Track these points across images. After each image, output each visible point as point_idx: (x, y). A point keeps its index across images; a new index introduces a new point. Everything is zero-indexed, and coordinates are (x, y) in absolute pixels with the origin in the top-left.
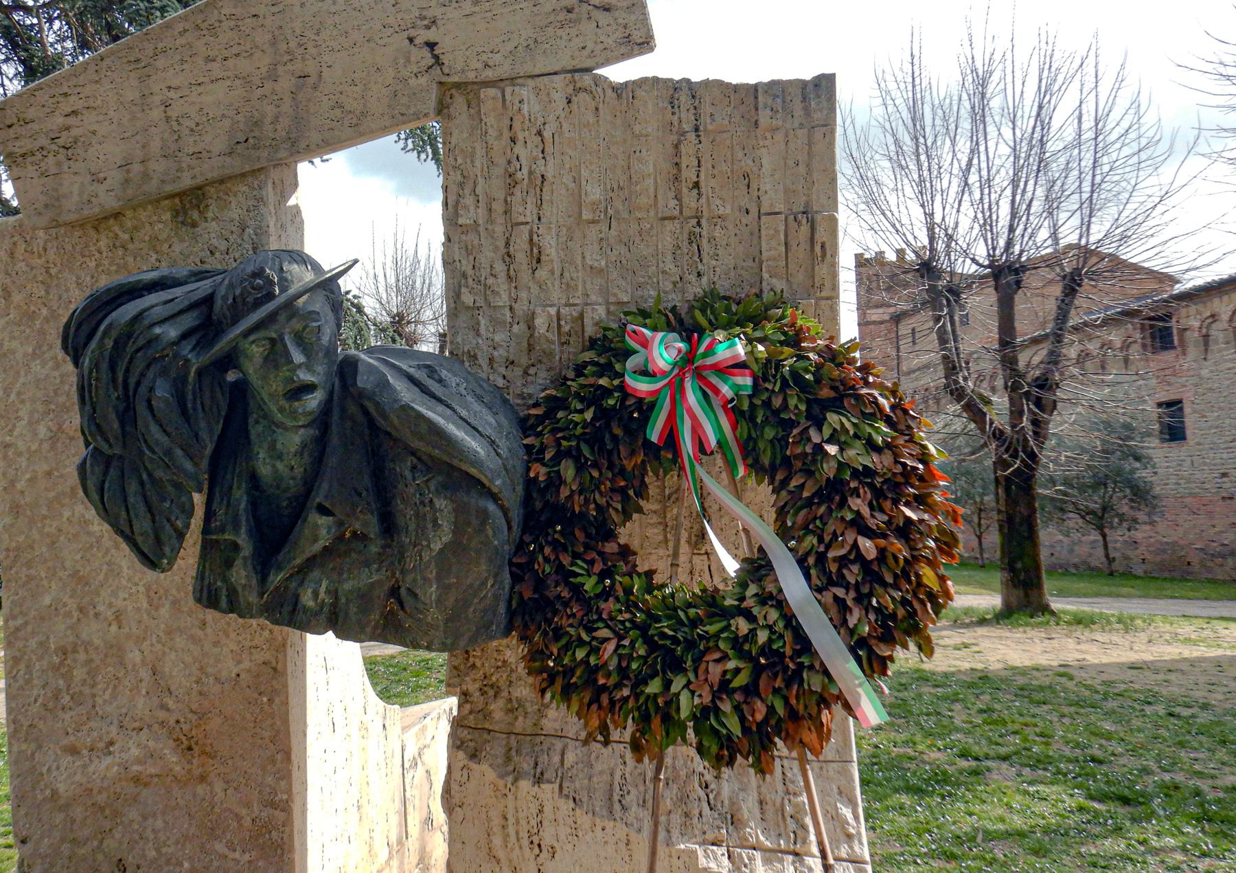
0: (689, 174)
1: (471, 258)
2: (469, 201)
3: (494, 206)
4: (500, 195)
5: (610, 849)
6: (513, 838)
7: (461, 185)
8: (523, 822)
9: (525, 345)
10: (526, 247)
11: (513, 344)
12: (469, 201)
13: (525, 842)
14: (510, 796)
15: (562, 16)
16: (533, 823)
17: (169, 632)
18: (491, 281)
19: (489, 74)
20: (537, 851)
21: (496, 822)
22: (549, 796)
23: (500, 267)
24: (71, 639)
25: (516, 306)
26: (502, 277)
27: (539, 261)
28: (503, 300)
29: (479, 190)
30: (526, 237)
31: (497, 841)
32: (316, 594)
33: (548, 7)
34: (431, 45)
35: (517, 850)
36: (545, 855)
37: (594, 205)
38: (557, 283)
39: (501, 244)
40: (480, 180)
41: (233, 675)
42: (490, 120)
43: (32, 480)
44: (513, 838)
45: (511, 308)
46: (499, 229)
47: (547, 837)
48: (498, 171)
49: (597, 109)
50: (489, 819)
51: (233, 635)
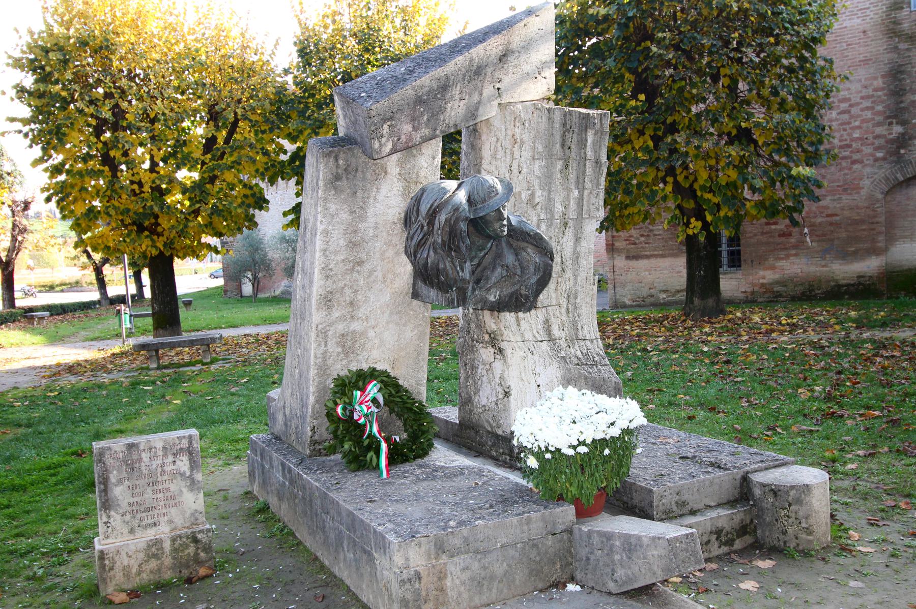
4: (510, 147)
21: (522, 368)
31: (523, 375)
42: (508, 118)
43: (337, 263)
47: (537, 371)
48: (509, 137)
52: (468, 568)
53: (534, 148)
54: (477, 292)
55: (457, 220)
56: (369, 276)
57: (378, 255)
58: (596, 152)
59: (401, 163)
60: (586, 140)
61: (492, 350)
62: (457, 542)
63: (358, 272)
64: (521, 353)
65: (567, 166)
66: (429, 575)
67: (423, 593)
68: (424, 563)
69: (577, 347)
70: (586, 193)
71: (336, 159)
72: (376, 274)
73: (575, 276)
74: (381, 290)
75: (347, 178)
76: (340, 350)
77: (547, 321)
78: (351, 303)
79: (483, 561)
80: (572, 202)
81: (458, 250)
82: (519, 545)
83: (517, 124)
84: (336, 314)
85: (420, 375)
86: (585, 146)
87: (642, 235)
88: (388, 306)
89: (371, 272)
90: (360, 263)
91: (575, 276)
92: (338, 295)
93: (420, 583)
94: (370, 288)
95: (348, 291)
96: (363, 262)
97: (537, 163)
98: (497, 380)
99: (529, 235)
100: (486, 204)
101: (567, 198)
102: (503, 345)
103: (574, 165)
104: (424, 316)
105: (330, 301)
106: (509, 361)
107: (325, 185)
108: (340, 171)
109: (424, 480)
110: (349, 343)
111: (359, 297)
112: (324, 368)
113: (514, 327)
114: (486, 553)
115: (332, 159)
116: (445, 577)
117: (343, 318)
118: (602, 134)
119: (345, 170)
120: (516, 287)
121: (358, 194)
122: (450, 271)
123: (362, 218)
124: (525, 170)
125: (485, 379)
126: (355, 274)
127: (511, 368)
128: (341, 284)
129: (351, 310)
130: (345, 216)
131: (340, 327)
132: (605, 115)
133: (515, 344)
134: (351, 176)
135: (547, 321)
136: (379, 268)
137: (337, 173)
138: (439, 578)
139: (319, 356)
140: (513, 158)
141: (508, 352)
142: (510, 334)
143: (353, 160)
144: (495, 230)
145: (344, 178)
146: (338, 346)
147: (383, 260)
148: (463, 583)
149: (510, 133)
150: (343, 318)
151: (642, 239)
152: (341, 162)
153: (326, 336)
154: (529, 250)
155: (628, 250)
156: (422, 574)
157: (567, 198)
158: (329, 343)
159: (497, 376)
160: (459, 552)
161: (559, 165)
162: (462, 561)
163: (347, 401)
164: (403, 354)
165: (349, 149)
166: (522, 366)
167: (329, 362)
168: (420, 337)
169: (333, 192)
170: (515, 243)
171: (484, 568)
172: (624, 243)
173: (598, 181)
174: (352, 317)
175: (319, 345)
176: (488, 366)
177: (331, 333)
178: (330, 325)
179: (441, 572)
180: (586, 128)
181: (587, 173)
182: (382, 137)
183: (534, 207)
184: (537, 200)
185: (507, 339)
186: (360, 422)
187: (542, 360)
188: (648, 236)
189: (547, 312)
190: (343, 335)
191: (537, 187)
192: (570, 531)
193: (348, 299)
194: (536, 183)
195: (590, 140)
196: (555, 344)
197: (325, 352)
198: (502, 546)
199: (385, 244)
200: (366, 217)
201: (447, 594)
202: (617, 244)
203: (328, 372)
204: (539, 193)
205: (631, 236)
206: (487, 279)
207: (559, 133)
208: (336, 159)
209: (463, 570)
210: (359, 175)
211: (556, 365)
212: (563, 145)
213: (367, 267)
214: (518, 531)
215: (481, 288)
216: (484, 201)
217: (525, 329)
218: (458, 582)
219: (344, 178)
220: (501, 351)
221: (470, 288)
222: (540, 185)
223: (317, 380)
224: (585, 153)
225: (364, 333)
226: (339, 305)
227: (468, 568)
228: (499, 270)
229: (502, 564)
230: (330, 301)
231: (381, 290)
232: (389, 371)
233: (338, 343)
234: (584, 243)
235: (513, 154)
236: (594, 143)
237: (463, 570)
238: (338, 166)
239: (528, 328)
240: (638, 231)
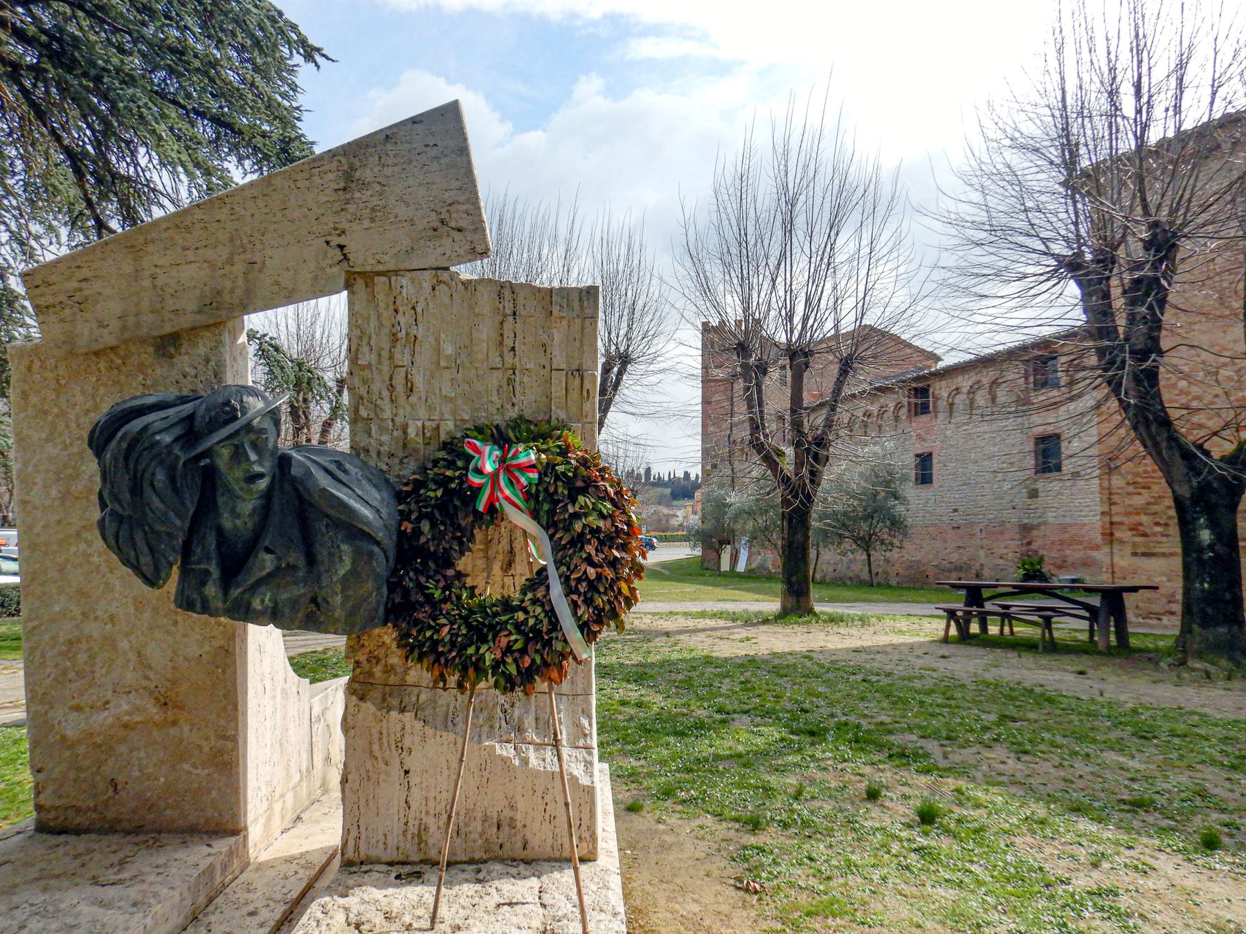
0: (509, 342)
2: (365, 349)
3: (383, 353)
5: (445, 747)
6: (386, 745)
7: (361, 338)
10: (404, 381)
12: (365, 349)
13: (393, 747)
15: (431, 233)
17: (150, 629)
18: (379, 402)
19: (381, 268)
21: (376, 736)
23: (386, 393)
26: (387, 399)
28: (387, 414)
29: (372, 343)
31: (376, 747)
34: (341, 247)
37: (448, 357)
39: (387, 378)
40: (374, 336)
42: (380, 297)
44: (386, 745)
45: (393, 420)
47: (407, 743)
50: (371, 735)
51: (197, 630)
87: (1157, 524)
151: (1158, 529)
155: (1134, 544)
166: (375, 731)
172: (1130, 533)
188: (1166, 525)
202: (1118, 534)
205: (1141, 524)
240: (1150, 517)
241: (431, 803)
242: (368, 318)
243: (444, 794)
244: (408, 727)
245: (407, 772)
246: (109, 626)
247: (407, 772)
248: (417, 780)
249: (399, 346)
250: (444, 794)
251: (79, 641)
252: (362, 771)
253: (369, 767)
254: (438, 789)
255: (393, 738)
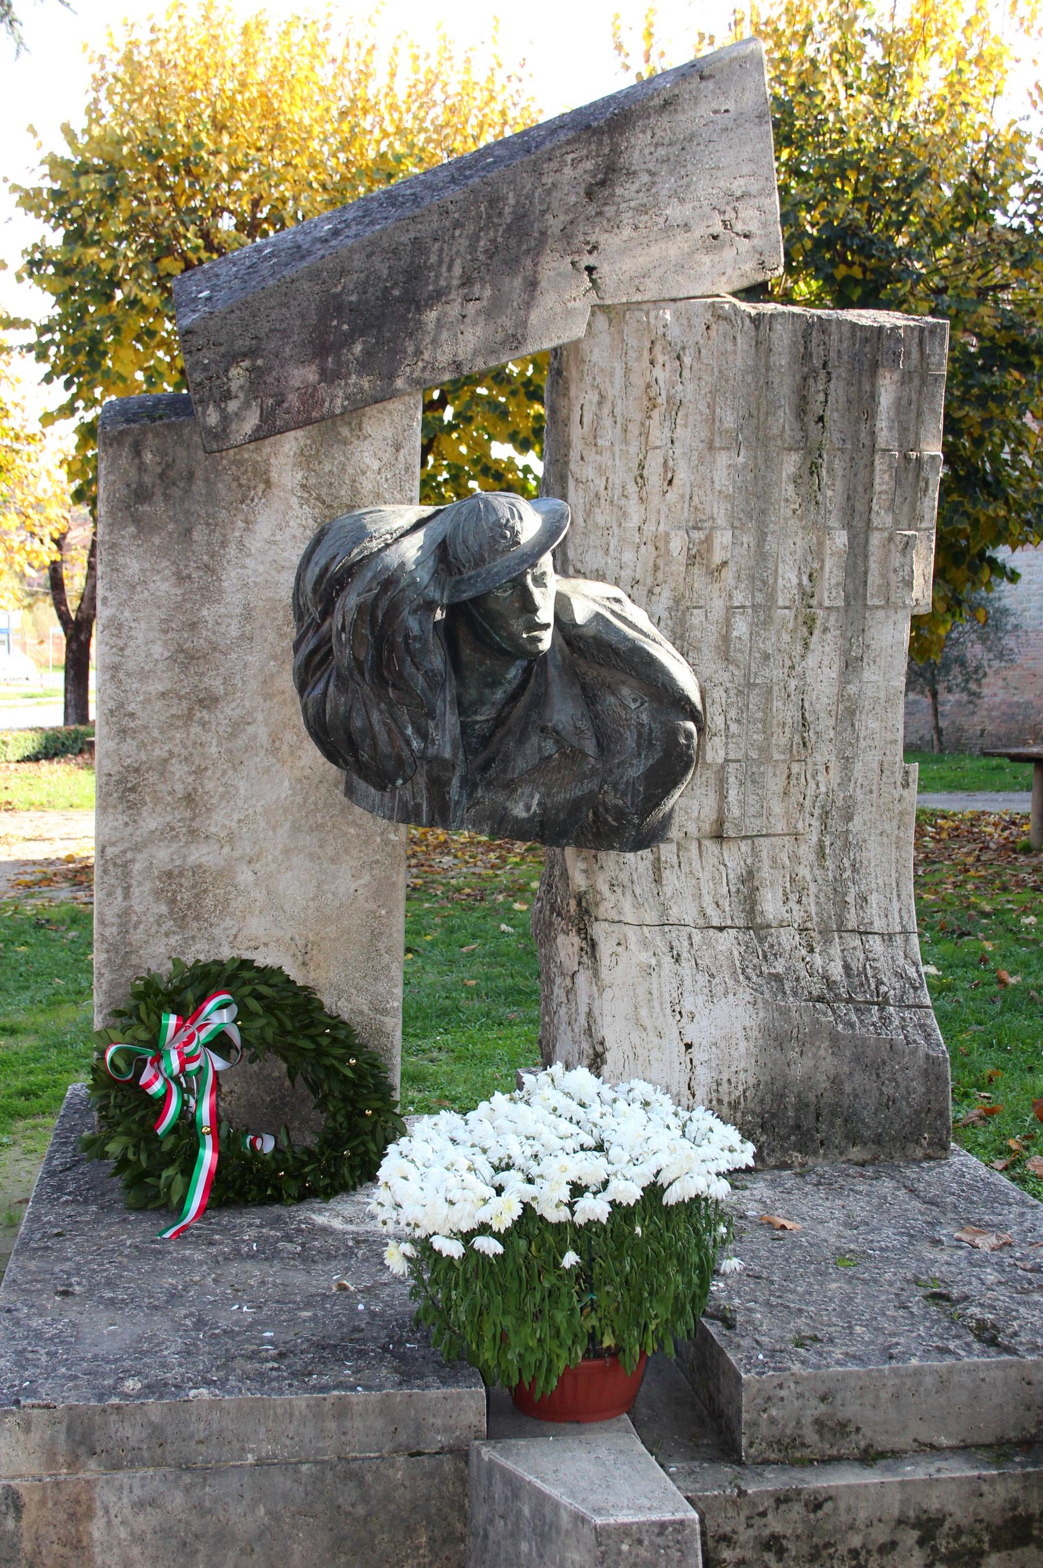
1: (604, 479)
2: (607, 422)
4: (638, 416)
6: (658, 1009)
8: (666, 996)
9: (651, 564)
10: (661, 470)
11: (639, 564)
12: (607, 422)
13: (669, 1011)
14: (654, 974)
16: (675, 995)
17: (287, 852)
20: (678, 1017)
21: (642, 995)
22: (688, 972)
23: (632, 489)
24: (178, 863)
25: (645, 527)
26: (634, 498)
27: (670, 482)
29: (617, 411)
30: (661, 460)
31: (644, 1012)
32: (528, 808)
33: (697, 234)
34: (590, 269)
35: (661, 1018)
36: (685, 1020)
38: (686, 505)
41: (352, 891)
42: (632, 342)
46: (633, 450)
47: (687, 1006)
49: (734, 338)
50: (636, 995)
51: (354, 852)
52: (153, 1502)
53: (712, 420)
54: (479, 793)
55: (393, 611)
56: (232, 736)
57: (254, 685)
58: (904, 429)
59: (306, 459)
60: (873, 397)
61: (576, 940)
62: (131, 1432)
63: (203, 724)
64: (645, 957)
65: (814, 469)
66: (43, 1502)
67: (27, 1546)
68: (36, 1471)
69: (835, 951)
70: (876, 539)
71: (137, 451)
72: (251, 729)
73: (847, 762)
74: (268, 771)
75: (167, 497)
76: (164, 909)
77: (749, 877)
78: (188, 799)
79: (197, 1492)
80: (828, 565)
81: (401, 683)
82: (304, 1468)
83: (660, 359)
84: (151, 822)
85: (381, 988)
86: (870, 414)
88: (286, 810)
89: (238, 726)
90: (209, 701)
91: (847, 762)
92: (152, 777)
93: (18, 1518)
94: (236, 765)
95: (178, 769)
96: (216, 700)
97: (723, 459)
98: (582, 1019)
99: (616, 652)
100: (483, 571)
101: (817, 552)
102: (599, 930)
103: (838, 465)
104: (387, 842)
105: (133, 789)
106: (604, 973)
107: (111, 513)
108: (147, 479)
109: (251, 1256)
110: (185, 896)
111: (210, 785)
112: (123, 950)
113: (644, 885)
114: (207, 1472)
115: (126, 451)
116: (89, 1514)
117: (168, 833)
118: (923, 382)
119: (162, 476)
120: (590, 785)
121: (196, 535)
122: (382, 737)
123: (210, 593)
124: (682, 476)
125: (563, 1011)
126: (195, 729)
127: (608, 994)
128: (159, 752)
129: (188, 814)
130: (163, 587)
131: (163, 855)
132: (933, 329)
133: (632, 934)
134: (176, 492)
135: (749, 877)
136: (260, 717)
137: (141, 485)
138: (72, 1516)
139: (110, 918)
140: (647, 448)
141: (605, 949)
142: (627, 904)
143: (181, 453)
144: (513, 638)
145: (158, 498)
146: (158, 900)
147: (267, 697)
148: (138, 1539)
149: (638, 381)
150: (168, 833)
152: (148, 457)
153: (127, 875)
154: (625, 691)
156: (26, 1499)
157: (817, 552)
158: (136, 891)
159: (583, 1009)
160: (135, 1461)
161: (791, 463)
162: (136, 1483)
163: (143, 1035)
164: (331, 930)
165: (168, 426)
166: (641, 991)
167: (137, 936)
168: (381, 891)
169: (132, 529)
170: (591, 673)
171: (200, 1510)
173: (913, 509)
174: (193, 832)
175: (109, 894)
176: (568, 981)
177: (137, 867)
178: (137, 848)
179: (78, 1502)
180: (875, 366)
181: (877, 488)
182: (227, 396)
183: (715, 572)
184: (717, 558)
185: (613, 915)
186: (151, 1091)
187: (702, 979)
189: (755, 853)
190: (169, 874)
191: (721, 522)
192: (461, 1453)
193: (179, 787)
194: (720, 511)
195: (886, 398)
196: (761, 940)
197: (125, 913)
198: (259, 1463)
199: (275, 657)
200: (221, 592)
201: (91, 1559)
203: (134, 960)
204: (723, 538)
206: (507, 760)
207: (788, 380)
208: (137, 451)
209: (140, 1505)
210: (199, 486)
211: (745, 995)
212: (801, 411)
213: (228, 711)
214: (309, 1431)
215: (489, 784)
216: (479, 561)
217: (678, 893)
218: (123, 1533)
219: (158, 498)
220: (592, 946)
221: (455, 782)
222: (731, 517)
223: (108, 976)
224: (873, 434)
225: (225, 874)
226: (157, 800)
227: (153, 1502)
228: (534, 740)
229: (253, 1508)
230: (133, 789)
231: (268, 771)
232: (287, 970)
233: (157, 893)
234: (870, 674)
235: (645, 434)
236: (900, 407)
237: (140, 1505)
238: (142, 468)
239: (688, 892)
241: (725, 1087)
242: (612, 375)
243: (742, 1076)
244: (688, 982)
245: (688, 1046)
246: (226, 850)
247: (688, 1046)
248: (704, 1057)
249: (655, 414)
250: (742, 1076)
251: (181, 874)
252: (626, 1046)
253: (636, 1040)
254: (733, 1069)
255: (667, 998)
